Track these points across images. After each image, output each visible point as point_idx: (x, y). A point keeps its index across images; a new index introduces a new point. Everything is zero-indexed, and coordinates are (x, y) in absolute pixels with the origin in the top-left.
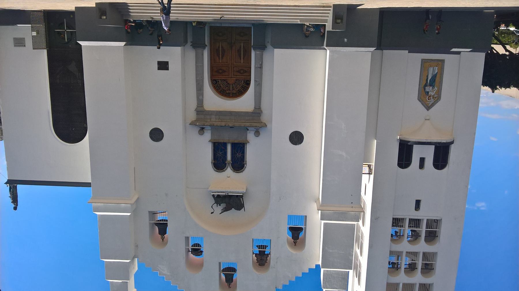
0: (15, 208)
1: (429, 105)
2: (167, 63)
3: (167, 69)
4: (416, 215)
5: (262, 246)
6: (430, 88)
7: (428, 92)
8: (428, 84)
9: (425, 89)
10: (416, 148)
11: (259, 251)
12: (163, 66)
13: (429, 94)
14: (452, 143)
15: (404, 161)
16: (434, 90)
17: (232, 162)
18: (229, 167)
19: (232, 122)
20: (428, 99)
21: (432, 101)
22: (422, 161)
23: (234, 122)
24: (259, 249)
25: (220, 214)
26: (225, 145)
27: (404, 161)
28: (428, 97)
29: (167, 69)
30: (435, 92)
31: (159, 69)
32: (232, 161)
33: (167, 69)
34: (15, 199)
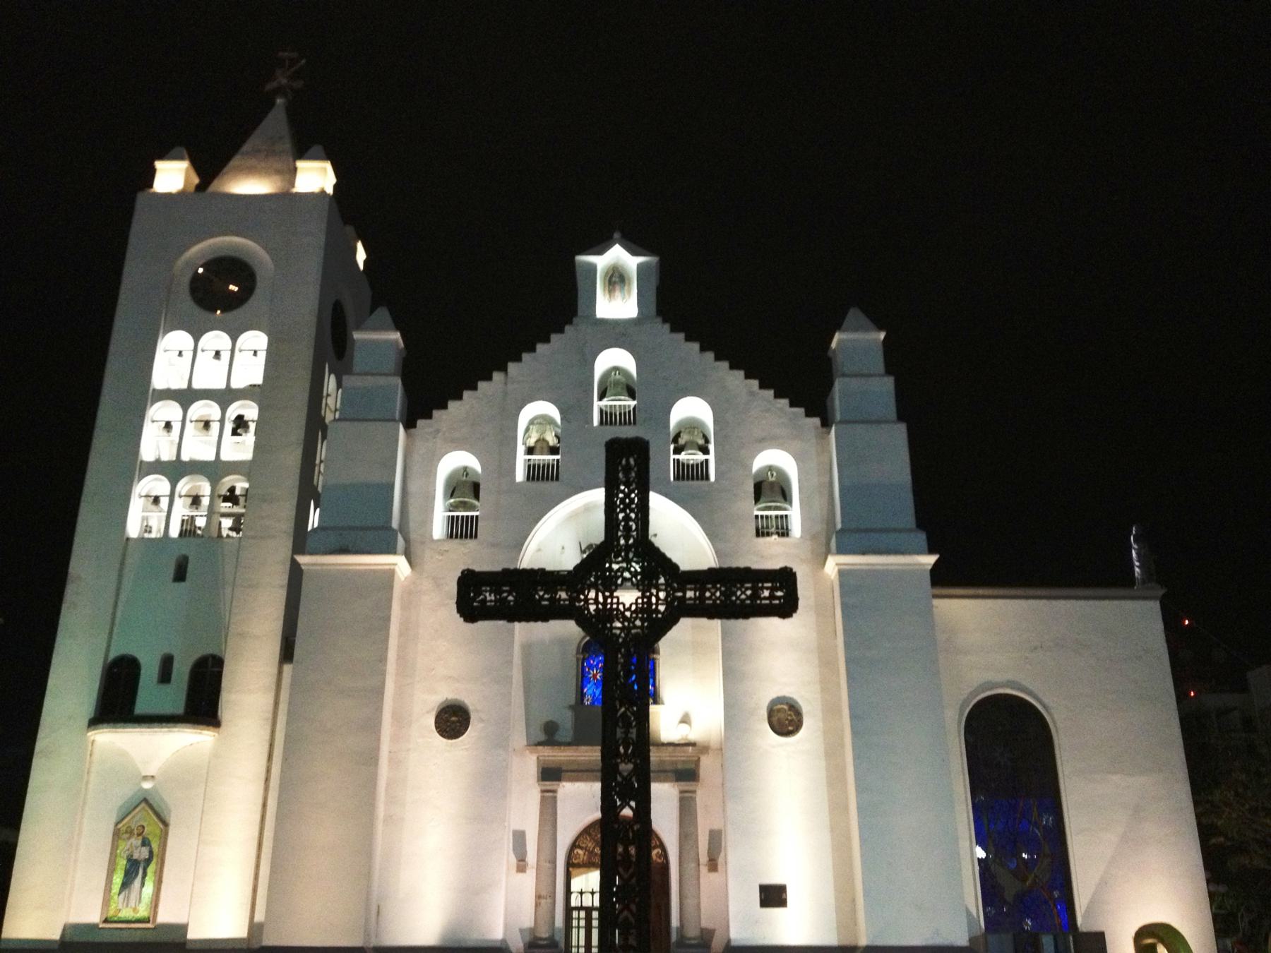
6: (138, 854)
9: (151, 852)
10: (180, 709)
12: (773, 896)
13: (139, 842)
16: (128, 850)
22: (165, 675)
28: (143, 832)
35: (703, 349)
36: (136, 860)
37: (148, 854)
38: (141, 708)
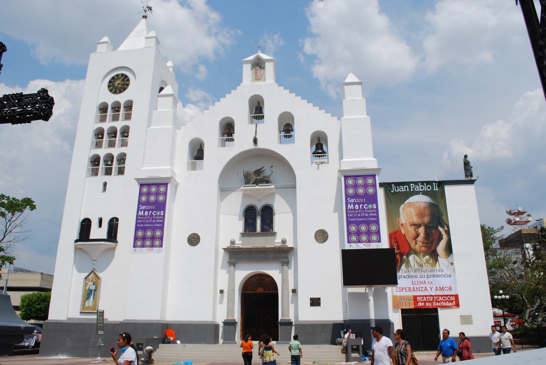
0: (466, 157)
1: (93, 273)
3: (310, 298)
4: (107, 178)
5: (230, 141)
7: (93, 284)
8: (93, 292)
9: (96, 287)
10: (105, 237)
11: (232, 136)
12: (315, 302)
13: (92, 283)
14: (76, 241)
15: (114, 224)
17: (256, 214)
18: (259, 209)
19: (254, 251)
20: (93, 278)
21: (90, 277)
23: (252, 251)
24: (232, 138)
25: (264, 167)
26: (263, 229)
27: (114, 224)
29: (312, 299)
30: (88, 285)
32: (256, 215)
33: (310, 298)
34: (467, 164)
35: (290, 92)
36: (91, 290)
37: (95, 287)
38: (91, 237)
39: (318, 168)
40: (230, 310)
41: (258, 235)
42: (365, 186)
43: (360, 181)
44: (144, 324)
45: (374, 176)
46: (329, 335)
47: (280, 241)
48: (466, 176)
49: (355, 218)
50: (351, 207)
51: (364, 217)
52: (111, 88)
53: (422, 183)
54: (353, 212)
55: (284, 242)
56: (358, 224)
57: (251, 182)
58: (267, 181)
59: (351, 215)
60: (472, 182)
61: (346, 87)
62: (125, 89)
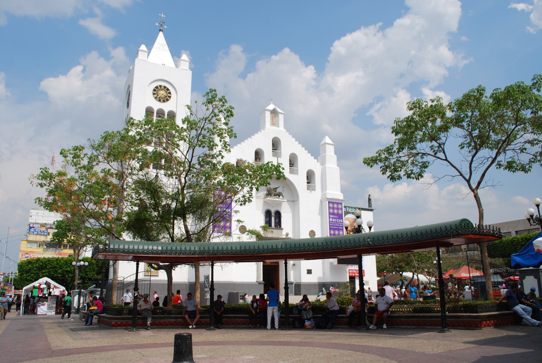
0: (369, 195)
2: (308, 273)
26: (275, 226)
29: (308, 270)
31: (311, 270)
39: (311, 192)
40: (258, 277)
41: (273, 229)
42: (338, 209)
43: (335, 206)
44: (224, 284)
45: (341, 204)
46: (317, 290)
47: (285, 234)
48: (369, 206)
49: (333, 226)
50: (331, 220)
51: (337, 226)
52: (156, 96)
53: (352, 208)
54: (332, 223)
55: (287, 235)
56: (334, 230)
57: (272, 195)
58: (279, 195)
59: (331, 225)
60: (372, 210)
61: (327, 145)
62: (167, 100)
